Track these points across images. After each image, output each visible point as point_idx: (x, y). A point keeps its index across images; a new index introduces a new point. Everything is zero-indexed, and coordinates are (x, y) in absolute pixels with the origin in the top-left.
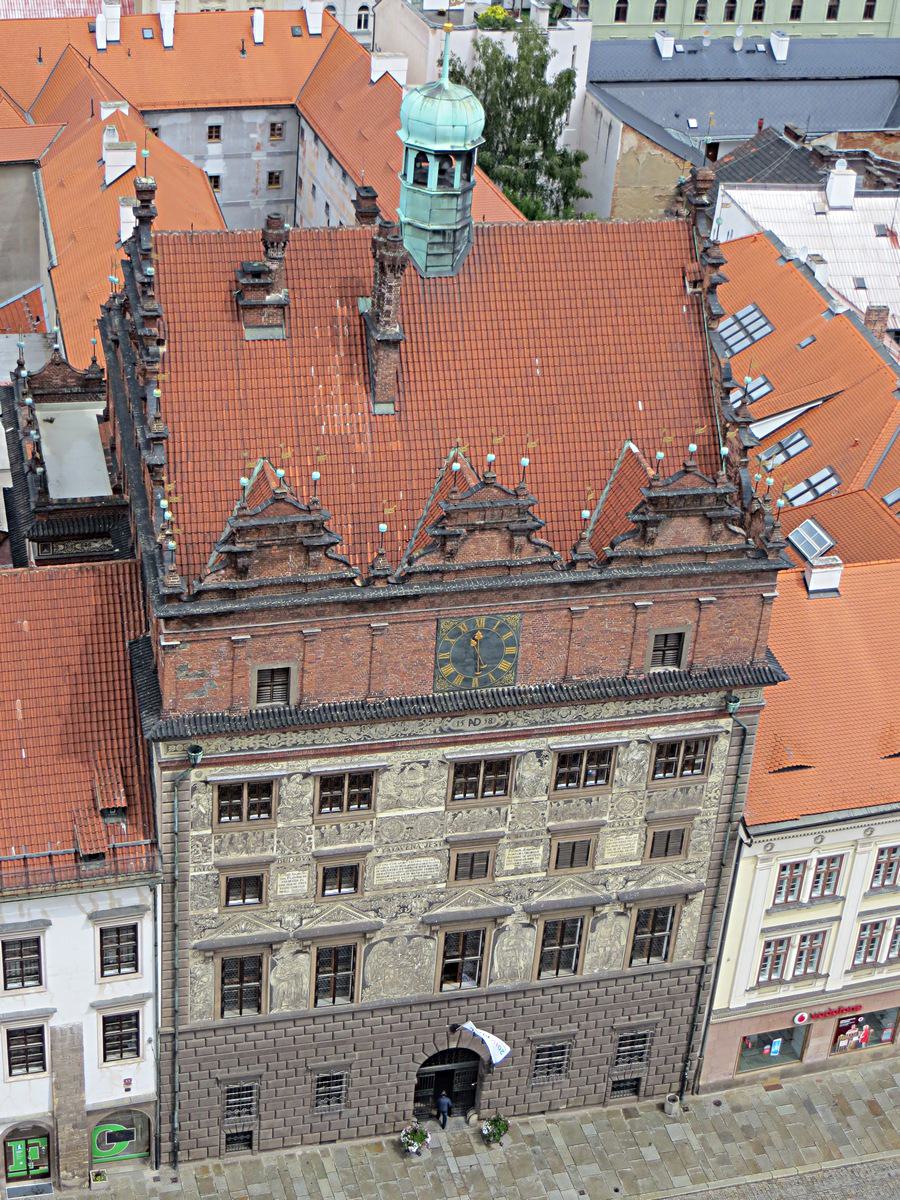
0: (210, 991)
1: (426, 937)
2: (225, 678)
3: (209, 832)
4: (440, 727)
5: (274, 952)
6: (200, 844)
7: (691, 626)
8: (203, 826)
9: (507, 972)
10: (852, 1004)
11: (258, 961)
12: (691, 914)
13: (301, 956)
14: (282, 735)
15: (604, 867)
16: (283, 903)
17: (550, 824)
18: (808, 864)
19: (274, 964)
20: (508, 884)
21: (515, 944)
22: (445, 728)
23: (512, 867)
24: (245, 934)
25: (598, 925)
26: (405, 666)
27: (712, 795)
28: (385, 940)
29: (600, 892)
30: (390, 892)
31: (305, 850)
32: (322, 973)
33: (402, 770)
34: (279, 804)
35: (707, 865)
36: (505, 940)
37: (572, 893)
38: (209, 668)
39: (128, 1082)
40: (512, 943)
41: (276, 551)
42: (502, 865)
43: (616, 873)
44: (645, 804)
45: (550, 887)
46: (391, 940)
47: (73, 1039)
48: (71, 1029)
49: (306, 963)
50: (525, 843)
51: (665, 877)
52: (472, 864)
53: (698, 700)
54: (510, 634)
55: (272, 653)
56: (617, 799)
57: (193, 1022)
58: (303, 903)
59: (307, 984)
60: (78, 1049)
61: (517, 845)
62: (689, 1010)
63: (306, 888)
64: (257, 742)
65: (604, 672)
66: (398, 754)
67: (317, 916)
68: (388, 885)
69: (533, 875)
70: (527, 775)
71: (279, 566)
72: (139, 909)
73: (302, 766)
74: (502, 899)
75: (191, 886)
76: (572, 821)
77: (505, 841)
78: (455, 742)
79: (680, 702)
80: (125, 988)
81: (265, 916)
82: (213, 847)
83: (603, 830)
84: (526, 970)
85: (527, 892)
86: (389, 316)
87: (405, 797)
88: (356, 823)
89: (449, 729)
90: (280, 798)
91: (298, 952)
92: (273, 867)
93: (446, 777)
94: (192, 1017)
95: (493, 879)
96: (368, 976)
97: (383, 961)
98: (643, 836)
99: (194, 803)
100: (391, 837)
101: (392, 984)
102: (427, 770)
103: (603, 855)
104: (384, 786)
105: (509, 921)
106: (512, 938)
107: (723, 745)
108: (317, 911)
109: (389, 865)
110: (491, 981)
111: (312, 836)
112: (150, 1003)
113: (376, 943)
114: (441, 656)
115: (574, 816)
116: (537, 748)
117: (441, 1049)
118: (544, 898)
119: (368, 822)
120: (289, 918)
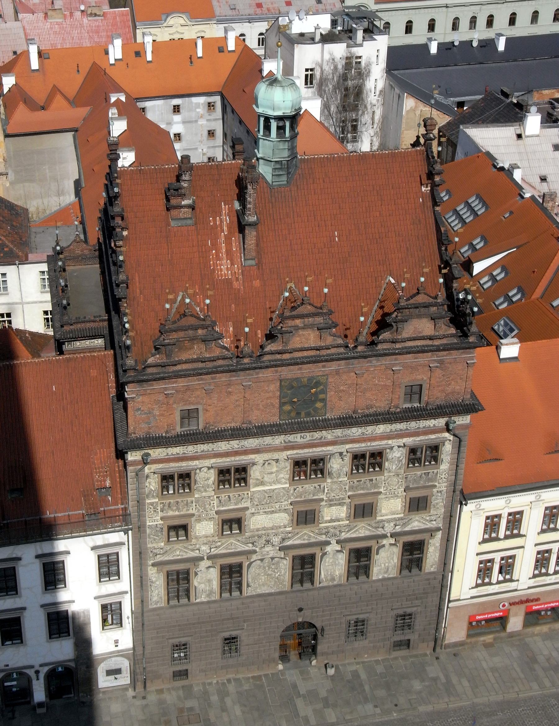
1: (282, 558)
3: (157, 500)
4: (284, 441)
5: (197, 566)
6: (152, 507)
7: (425, 380)
8: (153, 496)
9: (329, 578)
11: (187, 572)
12: (434, 545)
13: (212, 569)
14: (195, 446)
16: (200, 540)
17: (350, 493)
18: (502, 516)
19: (196, 574)
20: (327, 528)
21: (333, 562)
22: (287, 441)
23: (329, 518)
24: (179, 557)
25: (380, 551)
26: (263, 406)
27: (443, 476)
28: (259, 560)
29: (380, 532)
30: (260, 532)
31: (211, 510)
32: (224, 579)
33: (264, 464)
34: (195, 484)
35: (442, 516)
36: (328, 560)
37: (364, 533)
38: (153, 409)
39: (116, 642)
40: (331, 561)
41: (187, 344)
42: (323, 517)
43: (389, 521)
44: (404, 482)
46: (262, 560)
48: (84, 612)
49: (214, 574)
50: (335, 505)
53: (431, 423)
54: (322, 387)
55: (187, 400)
56: (387, 479)
58: (211, 539)
59: (215, 585)
61: (331, 505)
62: (436, 600)
63: (212, 530)
64: (181, 450)
65: (376, 407)
66: (261, 455)
67: (219, 546)
68: (259, 529)
69: (341, 523)
71: (189, 352)
73: (208, 462)
74: (324, 536)
75: (148, 531)
76: (362, 492)
77: (323, 503)
78: (292, 448)
79: (421, 424)
80: (111, 587)
81: (190, 547)
82: (159, 509)
83: (380, 497)
84: (340, 577)
85: (338, 532)
86: (250, 211)
87: (266, 479)
89: (289, 441)
90: (196, 481)
91: (209, 567)
92: (193, 519)
93: (289, 468)
94: (151, 604)
95: (318, 526)
97: (257, 571)
98: (404, 500)
99: (147, 484)
100: (260, 502)
101: (263, 585)
102: (278, 464)
103: (381, 511)
104: (254, 473)
105: (328, 549)
106: (331, 558)
107: (447, 449)
108: (219, 544)
110: (320, 583)
111: (215, 502)
113: (254, 562)
114: (283, 400)
115: (363, 489)
116: (340, 451)
117: (293, 622)
118: (349, 535)
120: (203, 548)
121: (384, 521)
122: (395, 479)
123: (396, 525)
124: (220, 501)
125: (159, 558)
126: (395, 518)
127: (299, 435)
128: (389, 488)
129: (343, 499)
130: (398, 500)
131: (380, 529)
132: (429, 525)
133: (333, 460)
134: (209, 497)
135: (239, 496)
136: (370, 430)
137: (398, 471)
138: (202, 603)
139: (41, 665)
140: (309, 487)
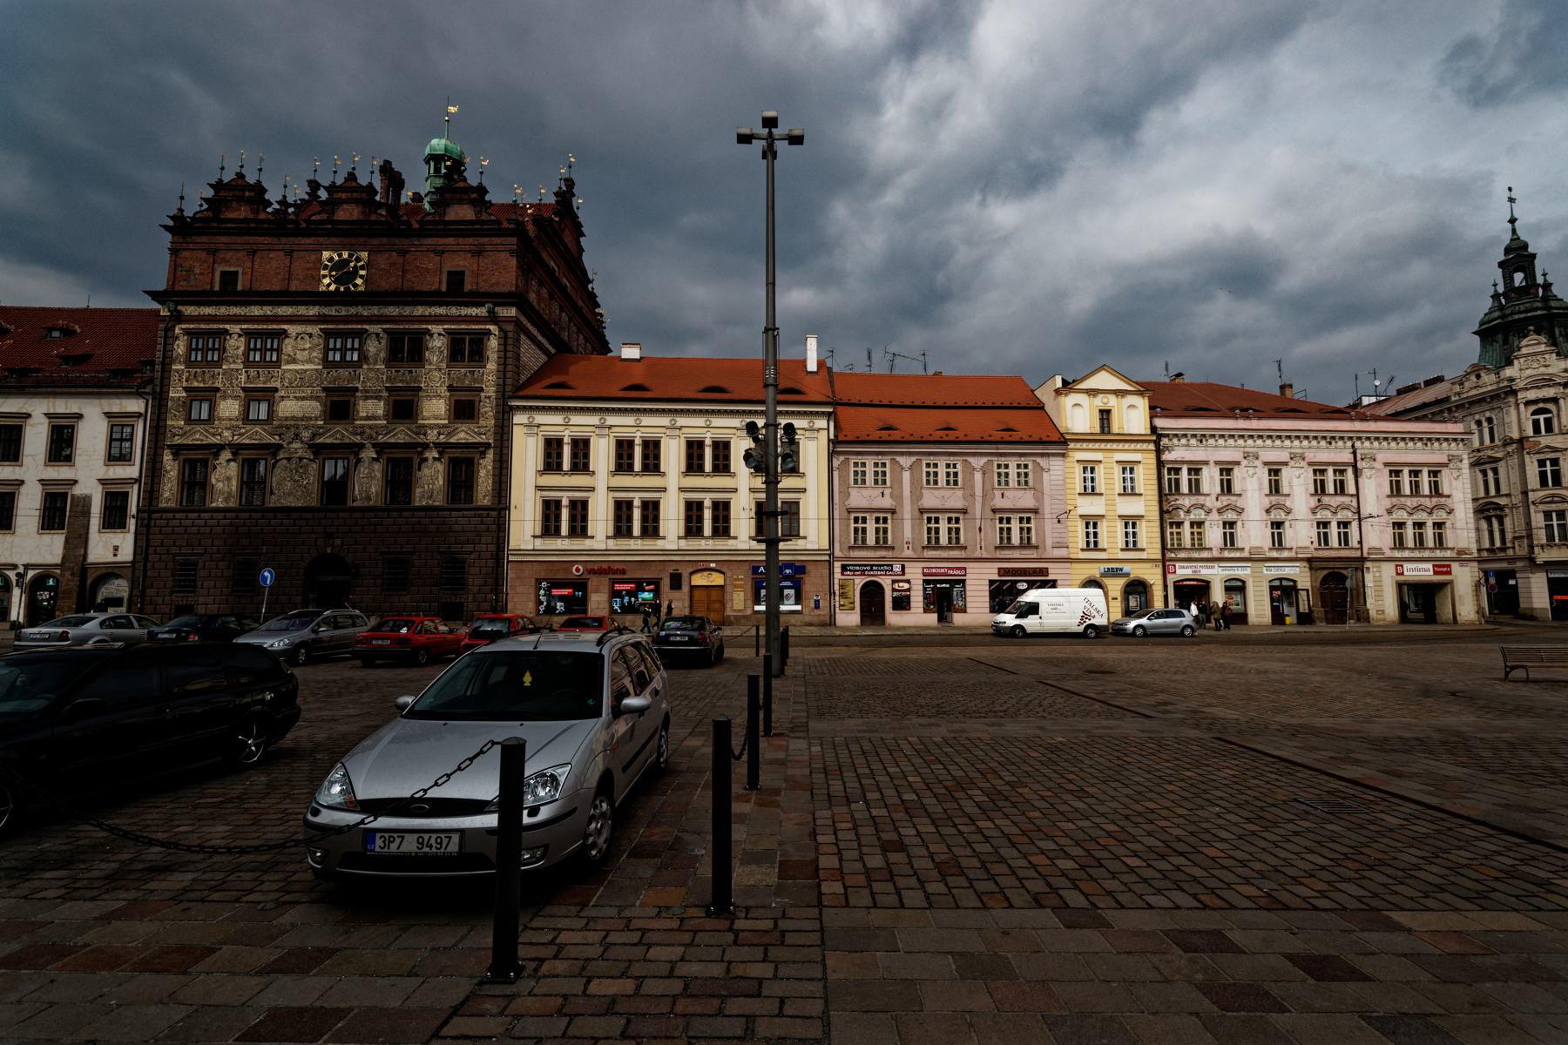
0: (175, 483)
2: (202, 274)
5: (217, 455)
10: (615, 567)
12: (485, 467)
13: (232, 463)
19: (215, 468)
20: (362, 426)
23: (364, 414)
29: (422, 439)
30: (288, 423)
33: (297, 338)
36: (363, 470)
39: (116, 548)
41: (234, 205)
42: (358, 412)
43: (432, 427)
45: (390, 432)
47: (83, 506)
50: (372, 398)
51: (463, 435)
52: (339, 406)
53: (474, 311)
54: (362, 263)
57: (163, 505)
60: (86, 513)
61: (367, 398)
67: (242, 434)
70: (371, 349)
72: (138, 415)
74: (359, 437)
75: (170, 404)
77: (359, 394)
84: (377, 495)
87: (298, 356)
92: (218, 395)
96: (274, 485)
105: (363, 455)
107: (493, 343)
108: (243, 431)
110: (353, 501)
112: (136, 487)
114: (322, 272)
115: (401, 381)
120: (226, 434)
123: (439, 434)
124: (248, 376)
125: (177, 441)
127: (334, 308)
129: (380, 391)
131: (422, 437)
132: (478, 440)
133: (369, 342)
134: (237, 370)
136: (407, 311)
138: (218, 510)
139: (27, 567)
140: (344, 372)
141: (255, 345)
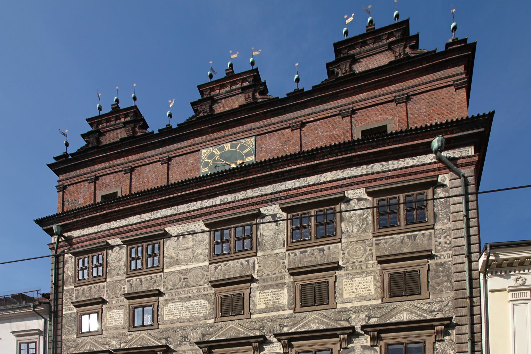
15: (344, 306)
43: (357, 311)
56: (347, 247)
88: (151, 277)
103: (341, 295)
109: (173, 305)
119: (158, 276)
121: (349, 310)
122: (358, 246)
126: (366, 306)
128: (351, 260)
130: (368, 278)
135: (152, 278)
137: (364, 234)
141: (136, 253)
